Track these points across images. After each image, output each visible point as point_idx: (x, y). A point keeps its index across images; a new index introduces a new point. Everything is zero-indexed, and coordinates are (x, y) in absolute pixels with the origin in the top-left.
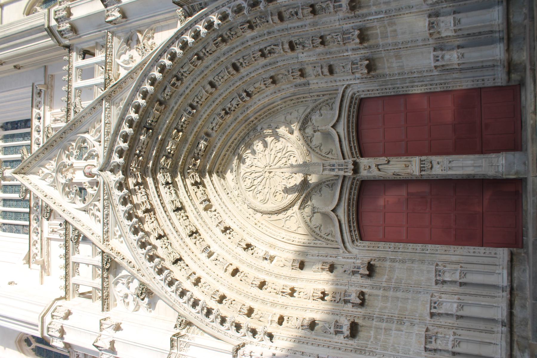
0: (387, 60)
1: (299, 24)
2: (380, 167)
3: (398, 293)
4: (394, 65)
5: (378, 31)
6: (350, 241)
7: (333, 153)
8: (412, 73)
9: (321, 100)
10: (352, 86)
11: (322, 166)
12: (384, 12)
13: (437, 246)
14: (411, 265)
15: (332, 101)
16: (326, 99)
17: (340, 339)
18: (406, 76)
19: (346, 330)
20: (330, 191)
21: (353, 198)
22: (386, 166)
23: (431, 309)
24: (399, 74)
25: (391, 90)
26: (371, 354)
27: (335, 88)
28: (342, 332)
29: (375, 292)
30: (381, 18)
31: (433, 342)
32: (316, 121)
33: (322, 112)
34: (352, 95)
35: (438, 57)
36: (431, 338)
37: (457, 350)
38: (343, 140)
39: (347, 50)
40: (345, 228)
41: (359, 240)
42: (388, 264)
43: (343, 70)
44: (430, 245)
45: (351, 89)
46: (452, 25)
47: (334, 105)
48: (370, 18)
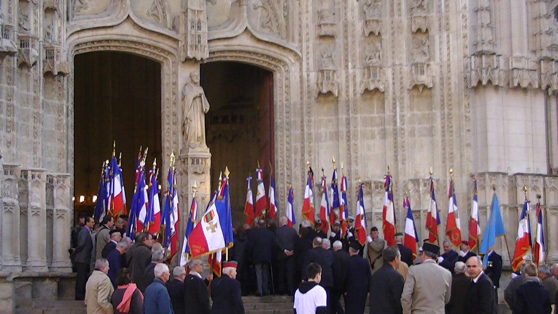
0: (330, 121)
2: (198, 100)
8: (310, 152)
10: (297, 64)
11: (199, 9)
12: (403, 127)
15: (275, 29)
16: (280, 21)
18: (306, 143)
20: (146, 11)
21: (139, 49)
22: (199, 109)
23: (32, 171)
24: (310, 134)
25: (285, 119)
27: (297, 37)
30: (395, 122)
33: (260, 10)
34: (284, 62)
38: (226, 43)
39: (354, 67)
40: (101, 35)
45: (293, 61)
47: (267, 30)
48: (398, 109)
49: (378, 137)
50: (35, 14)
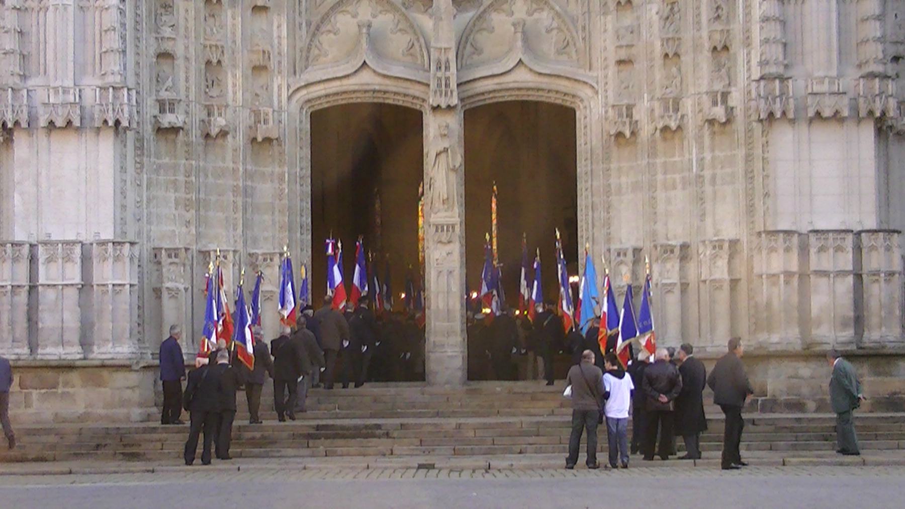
1: (704, 19)
2: (443, 156)
3: (231, 194)
4: (624, 179)
5: (677, 159)
6: (310, 96)
7: (475, 57)
9: (575, 34)
13: (310, 250)
14: (277, 210)
17: (151, 109)
19: (168, 119)
26: (138, 166)
28: (162, 111)
29: (229, 155)
31: (170, 260)
32: (537, 21)
33: (555, 32)
35: (625, 255)
36: (176, 256)
37: (165, 295)
38: (496, 80)
40: (334, 87)
41: (312, 109)
42: (277, 170)
43: (623, 86)
44: (310, 237)
46: (664, 281)
49: (680, 186)
50: (234, 76)
